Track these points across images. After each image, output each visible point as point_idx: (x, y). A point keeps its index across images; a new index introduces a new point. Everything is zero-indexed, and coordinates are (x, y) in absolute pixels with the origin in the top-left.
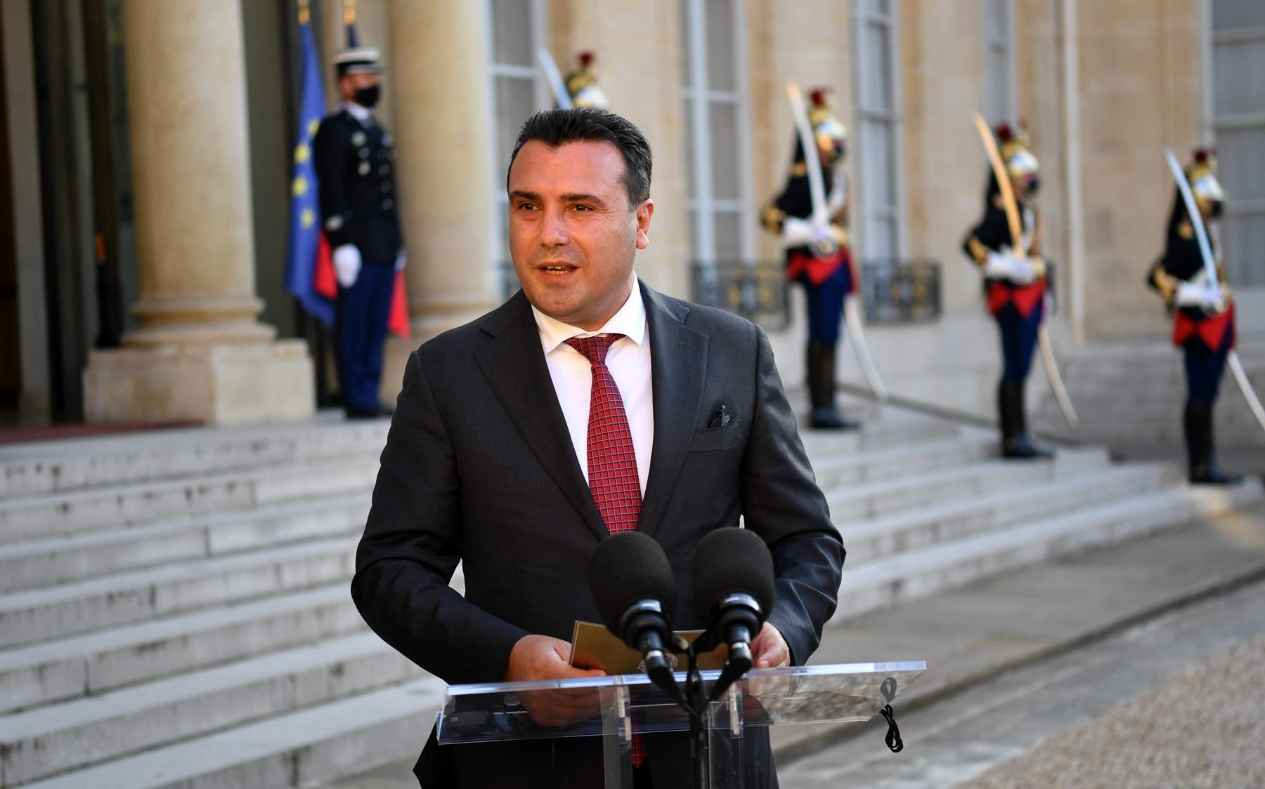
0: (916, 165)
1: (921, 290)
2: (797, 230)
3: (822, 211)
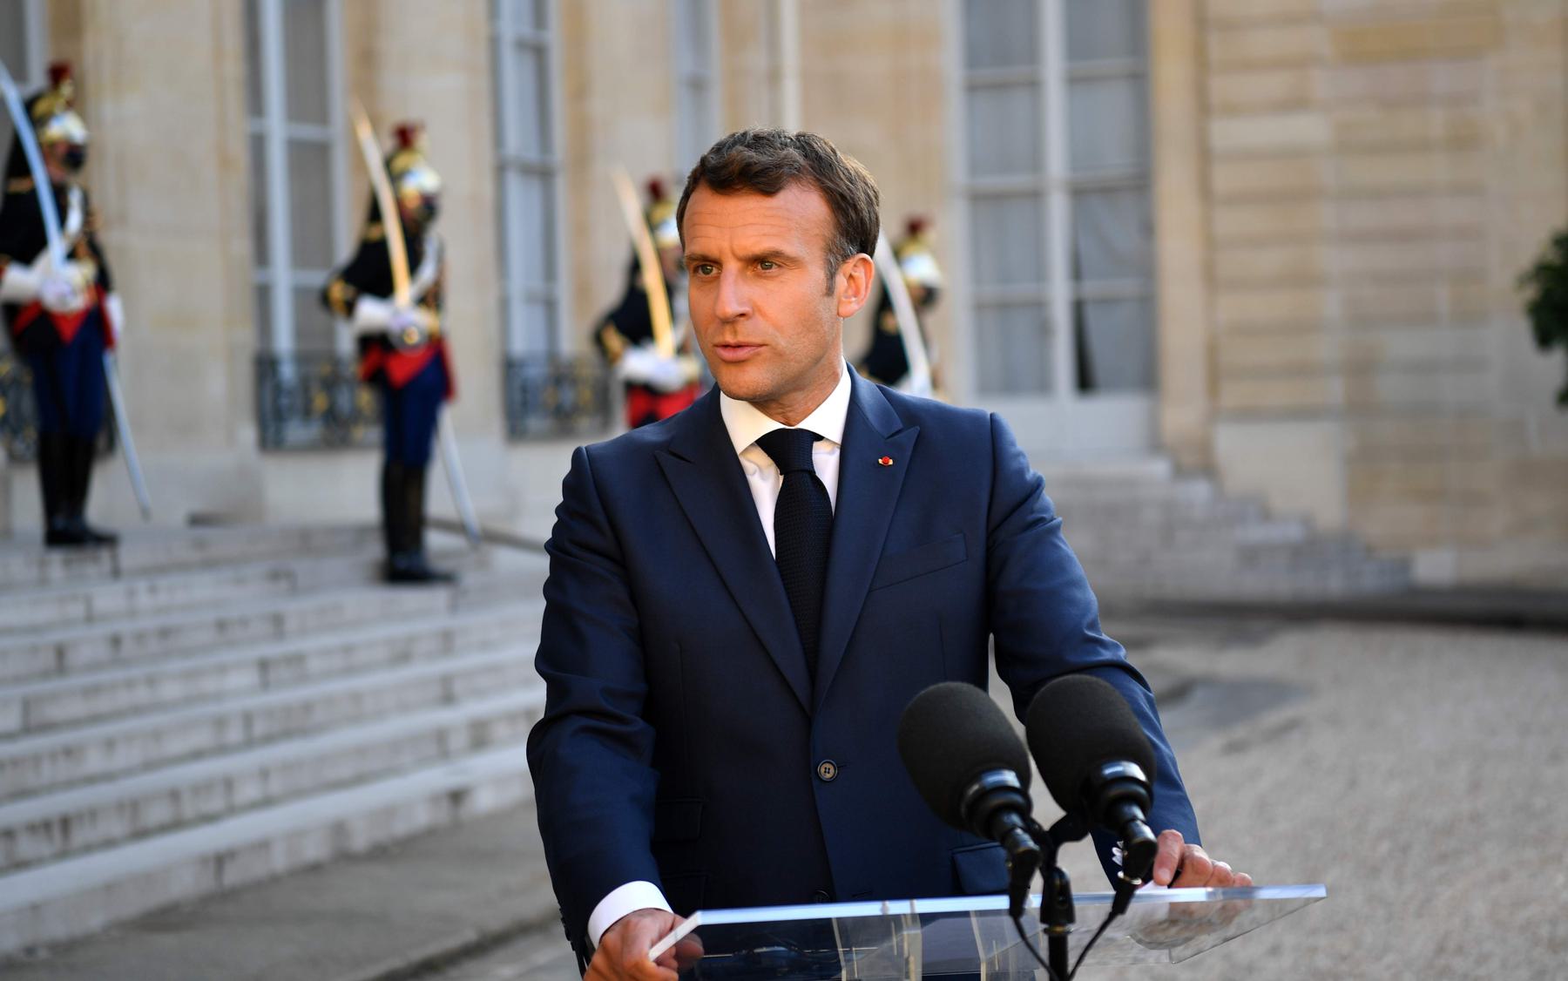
0: (582, 230)
1: (587, 395)
2: (371, 313)
3: (405, 290)
